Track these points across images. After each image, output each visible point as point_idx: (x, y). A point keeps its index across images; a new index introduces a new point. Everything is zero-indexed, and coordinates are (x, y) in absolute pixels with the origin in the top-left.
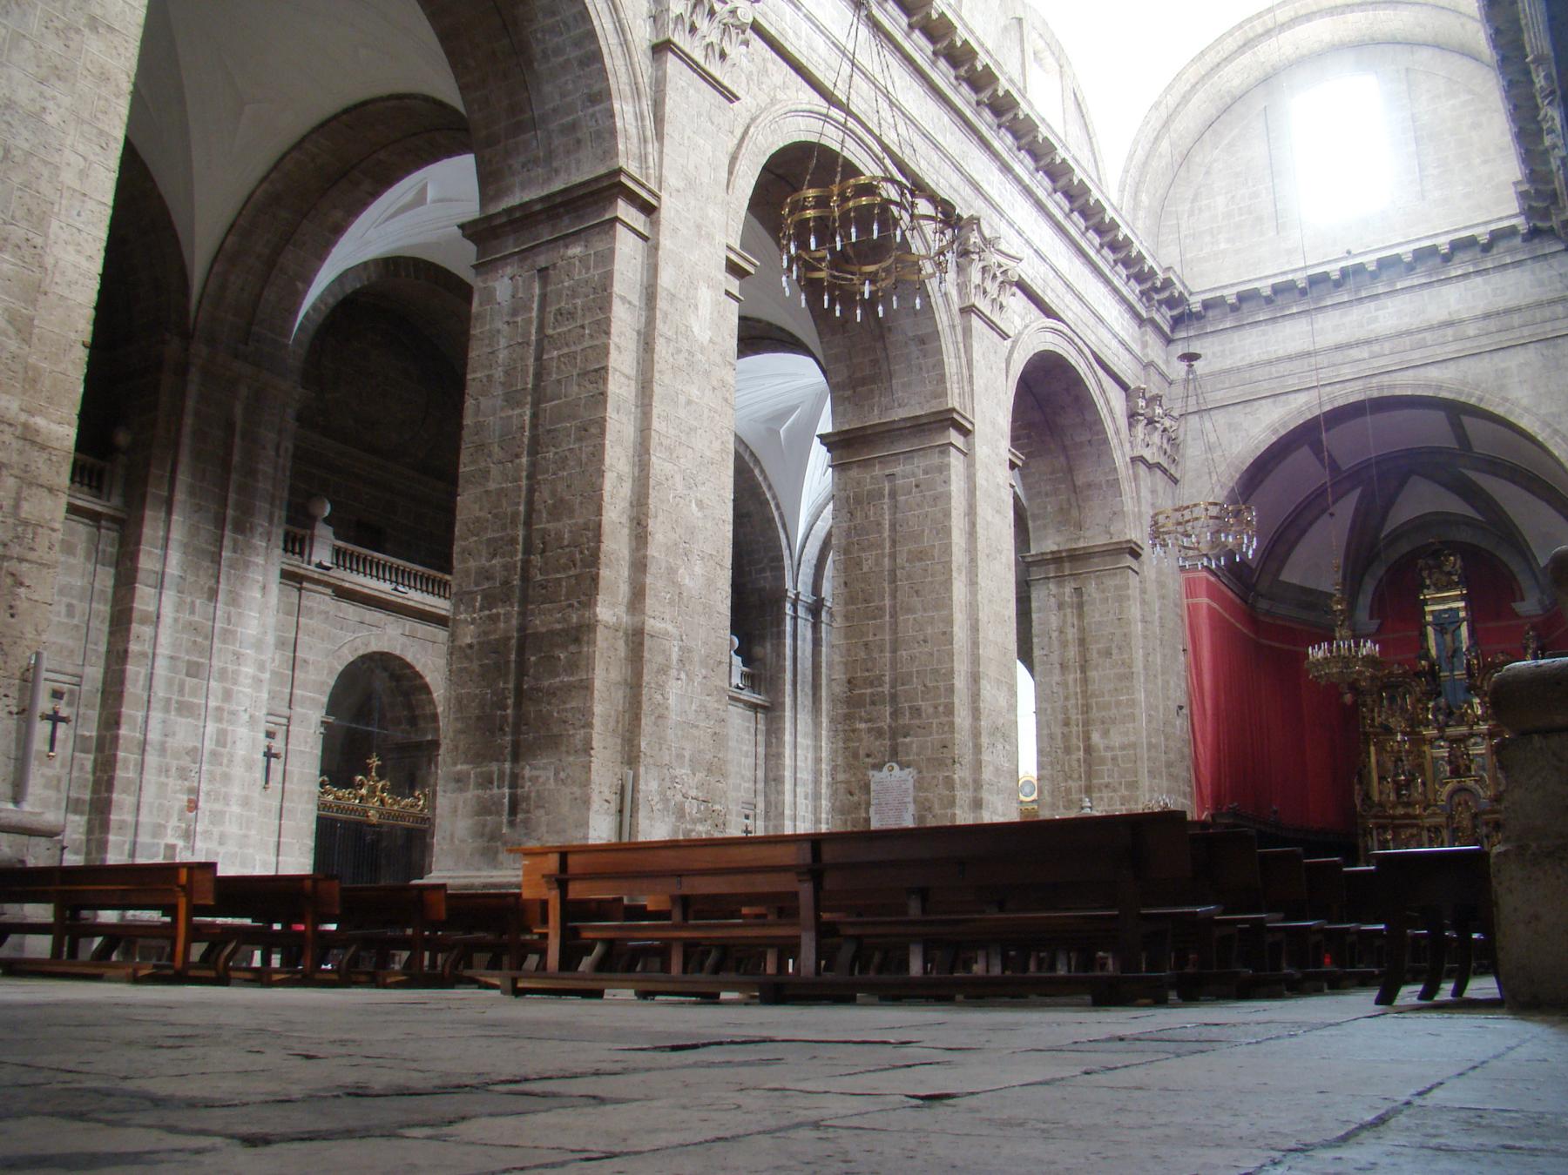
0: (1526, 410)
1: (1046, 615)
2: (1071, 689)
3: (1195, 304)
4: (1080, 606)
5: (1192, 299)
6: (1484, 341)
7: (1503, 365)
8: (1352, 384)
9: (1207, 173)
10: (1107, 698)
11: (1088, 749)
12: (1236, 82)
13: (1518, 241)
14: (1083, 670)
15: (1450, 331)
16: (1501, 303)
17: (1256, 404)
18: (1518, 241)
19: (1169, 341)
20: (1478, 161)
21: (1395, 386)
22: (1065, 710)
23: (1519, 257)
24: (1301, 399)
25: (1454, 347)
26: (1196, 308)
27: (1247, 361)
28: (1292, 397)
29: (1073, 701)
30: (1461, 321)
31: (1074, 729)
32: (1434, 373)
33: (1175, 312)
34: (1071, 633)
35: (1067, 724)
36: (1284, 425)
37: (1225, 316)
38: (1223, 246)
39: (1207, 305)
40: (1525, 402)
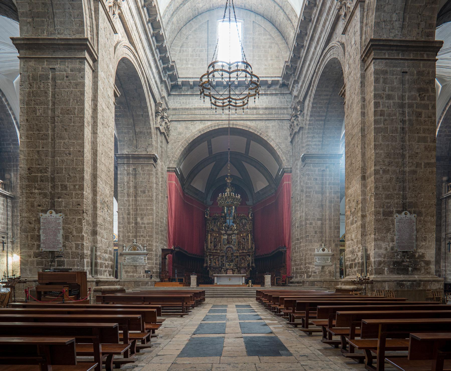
0: (273, 139)
1: (123, 178)
2: (131, 203)
3: (180, 81)
4: (135, 175)
5: (179, 80)
6: (264, 116)
7: (268, 125)
8: (225, 121)
9: (187, 38)
10: (143, 207)
11: (136, 223)
12: (201, 5)
13: (278, 87)
14: (135, 197)
15: (255, 111)
16: (270, 105)
17: (195, 122)
18: (278, 87)
19: (169, 95)
20: (269, 59)
21: (237, 125)
22: (128, 210)
23: (277, 92)
24: (209, 123)
25: (255, 116)
26: (180, 83)
27: (194, 107)
28: (206, 122)
29: (131, 207)
30: (259, 108)
31: (131, 216)
32: (249, 123)
33: (172, 83)
34: (131, 184)
35: (129, 214)
36: (203, 130)
37: (188, 90)
38: (189, 66)
39: (184, 84)
40: (272, 137)
